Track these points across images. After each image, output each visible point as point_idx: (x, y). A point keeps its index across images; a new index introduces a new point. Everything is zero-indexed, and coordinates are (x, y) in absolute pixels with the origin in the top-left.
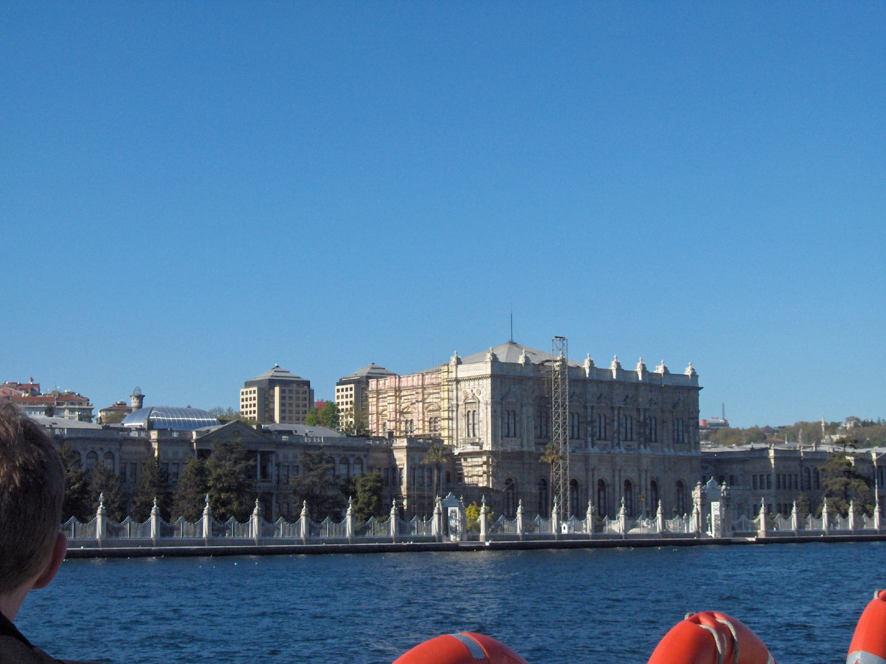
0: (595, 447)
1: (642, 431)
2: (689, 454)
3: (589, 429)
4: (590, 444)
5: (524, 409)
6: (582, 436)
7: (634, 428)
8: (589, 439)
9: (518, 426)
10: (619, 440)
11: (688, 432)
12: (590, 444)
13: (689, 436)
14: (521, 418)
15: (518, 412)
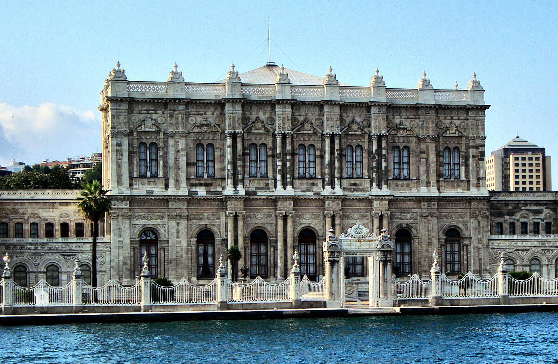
0: (289, 187)
1: (374, 164)
2: (467, 194)
3: (279, 163)
4: (279, 183)
5: (171, 142)
6: (270, 174)
7: (365, 161)
8: (279, 177)
9: (161, 163)
10: (332, 177)
11: (467, 166)
12: (279, 183)
13: (467, 172)
14: (166, 153)
15: (161, 144)
